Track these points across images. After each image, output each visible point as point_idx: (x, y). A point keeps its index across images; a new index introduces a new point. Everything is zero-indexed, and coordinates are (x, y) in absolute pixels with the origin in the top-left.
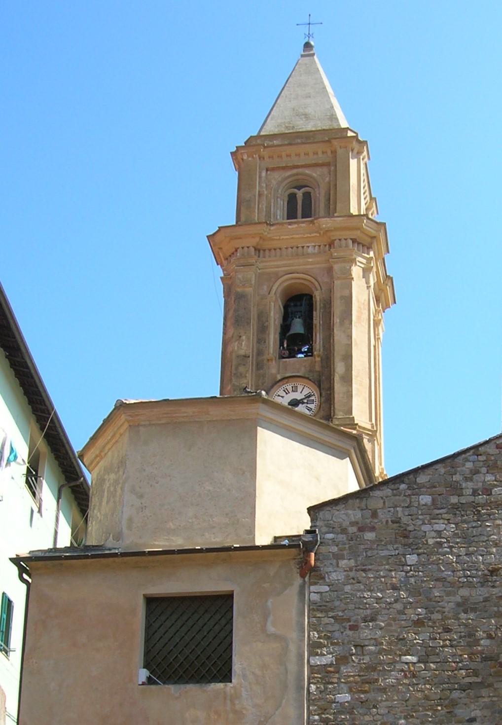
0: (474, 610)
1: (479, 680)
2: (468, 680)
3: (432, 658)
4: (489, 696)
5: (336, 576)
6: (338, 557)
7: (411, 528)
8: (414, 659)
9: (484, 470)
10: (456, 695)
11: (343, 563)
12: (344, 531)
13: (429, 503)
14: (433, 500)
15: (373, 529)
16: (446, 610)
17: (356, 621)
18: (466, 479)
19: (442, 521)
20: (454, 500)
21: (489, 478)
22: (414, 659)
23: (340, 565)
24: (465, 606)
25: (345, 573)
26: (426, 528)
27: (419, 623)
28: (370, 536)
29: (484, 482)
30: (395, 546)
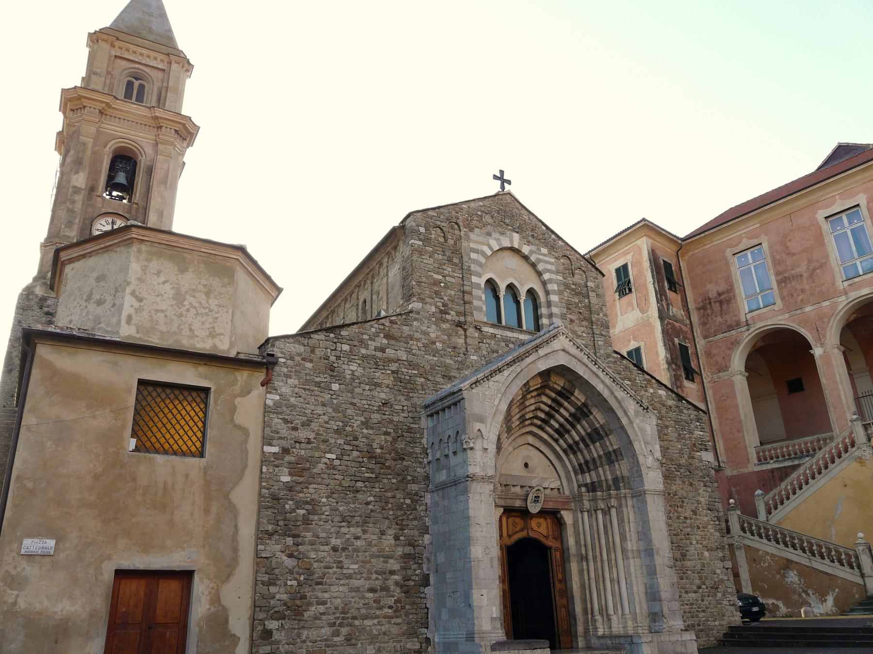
0: (372, 428)
1: (374, 476)
2: (366, 475)
3: (346, 458)
4: (379, 488)
5: (285, 390)
6: (288, 376)
7: (336, 365)
8: (333, 456)
9: (382, 335)
10: (359, 484)
11: (290, 381)
12: (292, 359)
13: (348, 350)
14: (350, 348)
15: (311, 361)
16: (355, 425)
17: (297, 424)
18: (370, 339)
19: (355, 364)
20: (363, 351)
21: (385, 341)
22: (333, 456)
23: (288, 382)
24: (366, 424)
25: (291, 389)
26: (344, 366)
27: (338, 432)
28: (309, 365)
29: (381, 343)
30: (325, 376)
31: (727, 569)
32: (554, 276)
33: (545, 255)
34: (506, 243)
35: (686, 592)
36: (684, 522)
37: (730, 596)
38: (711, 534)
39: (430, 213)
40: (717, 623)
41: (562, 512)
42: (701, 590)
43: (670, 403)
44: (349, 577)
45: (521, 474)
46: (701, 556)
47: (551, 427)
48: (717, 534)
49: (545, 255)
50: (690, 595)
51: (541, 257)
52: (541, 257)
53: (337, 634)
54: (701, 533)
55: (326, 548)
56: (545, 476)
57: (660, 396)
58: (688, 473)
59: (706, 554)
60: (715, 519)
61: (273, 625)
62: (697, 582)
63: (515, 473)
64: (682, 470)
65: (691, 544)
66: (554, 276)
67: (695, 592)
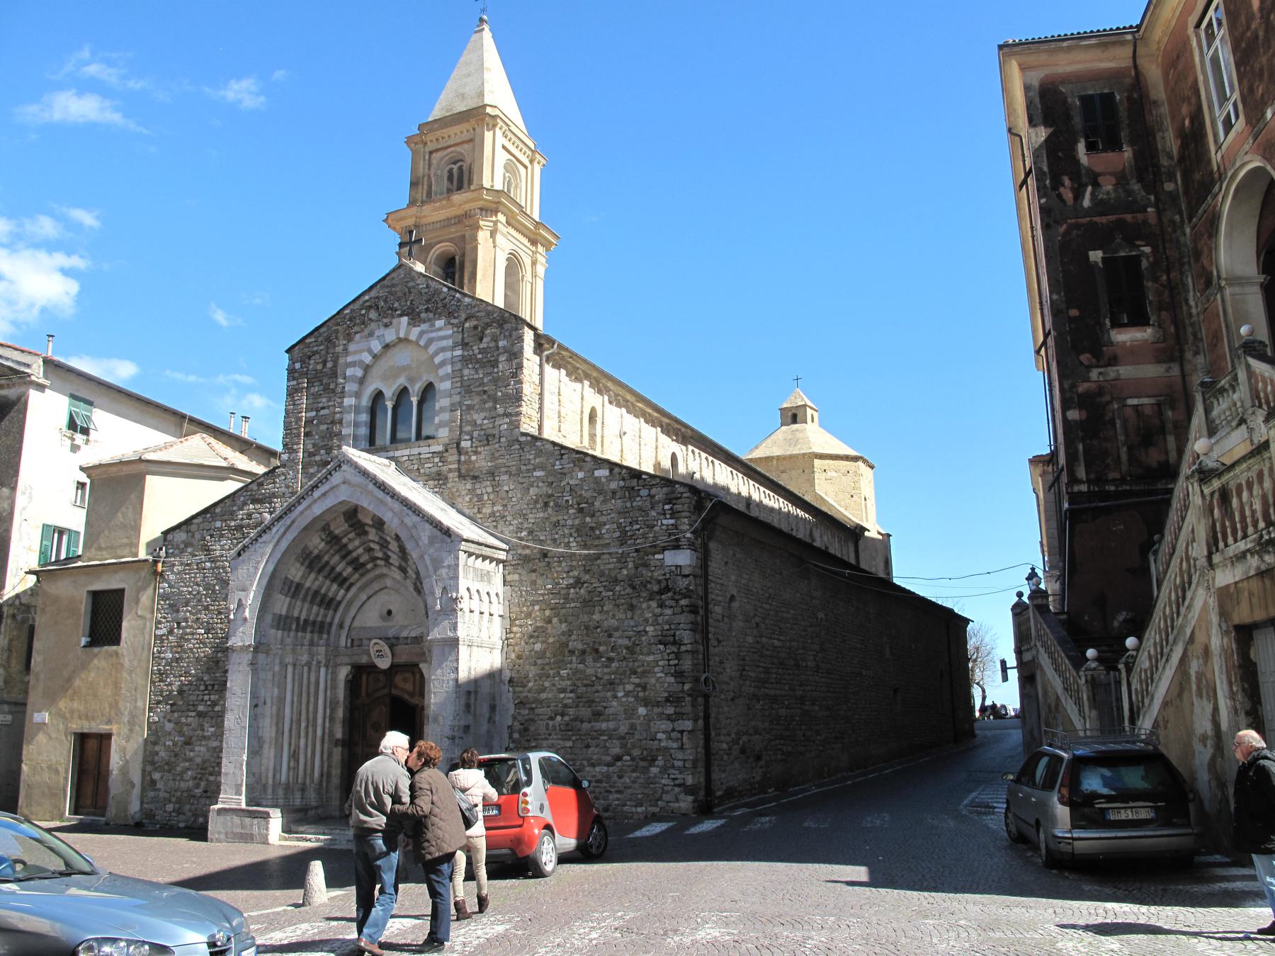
8: (203, 631)
31: (682, 732)
32: (449, 355)
33: (440, 329)
34: (390, 335)
35: (593, 765)
36: (607, 667)
37: (676, 772)
38: (657, 680)
39: (308, 341)
40: (639, 810)
41: (421, 665)
42: (619, 764)
43: (613, 485)
44: (208, 738)
45: (377, 625)
46: (630, 713)
47: (351, 575)
48: (672, 680)
49: (440, 329)
50: (598, 769)
51: (434, 335)
52: (434, 335)
53: (198, 786)
54: (637, 681)
55: (193, 714)
56: (406, 623)
57: (597, 481)
58: (629, 590)
59: (642, 711)
60: (672, 656)
61: (157, 776)
62: (616, 750)
63: (370, 624)
64: (618, 588)
65: (615, 697)
66: (449, 355)
67: (609, 765)
